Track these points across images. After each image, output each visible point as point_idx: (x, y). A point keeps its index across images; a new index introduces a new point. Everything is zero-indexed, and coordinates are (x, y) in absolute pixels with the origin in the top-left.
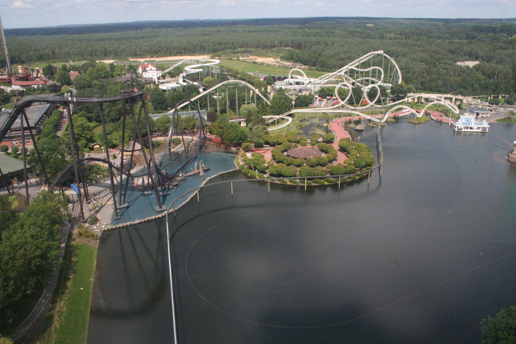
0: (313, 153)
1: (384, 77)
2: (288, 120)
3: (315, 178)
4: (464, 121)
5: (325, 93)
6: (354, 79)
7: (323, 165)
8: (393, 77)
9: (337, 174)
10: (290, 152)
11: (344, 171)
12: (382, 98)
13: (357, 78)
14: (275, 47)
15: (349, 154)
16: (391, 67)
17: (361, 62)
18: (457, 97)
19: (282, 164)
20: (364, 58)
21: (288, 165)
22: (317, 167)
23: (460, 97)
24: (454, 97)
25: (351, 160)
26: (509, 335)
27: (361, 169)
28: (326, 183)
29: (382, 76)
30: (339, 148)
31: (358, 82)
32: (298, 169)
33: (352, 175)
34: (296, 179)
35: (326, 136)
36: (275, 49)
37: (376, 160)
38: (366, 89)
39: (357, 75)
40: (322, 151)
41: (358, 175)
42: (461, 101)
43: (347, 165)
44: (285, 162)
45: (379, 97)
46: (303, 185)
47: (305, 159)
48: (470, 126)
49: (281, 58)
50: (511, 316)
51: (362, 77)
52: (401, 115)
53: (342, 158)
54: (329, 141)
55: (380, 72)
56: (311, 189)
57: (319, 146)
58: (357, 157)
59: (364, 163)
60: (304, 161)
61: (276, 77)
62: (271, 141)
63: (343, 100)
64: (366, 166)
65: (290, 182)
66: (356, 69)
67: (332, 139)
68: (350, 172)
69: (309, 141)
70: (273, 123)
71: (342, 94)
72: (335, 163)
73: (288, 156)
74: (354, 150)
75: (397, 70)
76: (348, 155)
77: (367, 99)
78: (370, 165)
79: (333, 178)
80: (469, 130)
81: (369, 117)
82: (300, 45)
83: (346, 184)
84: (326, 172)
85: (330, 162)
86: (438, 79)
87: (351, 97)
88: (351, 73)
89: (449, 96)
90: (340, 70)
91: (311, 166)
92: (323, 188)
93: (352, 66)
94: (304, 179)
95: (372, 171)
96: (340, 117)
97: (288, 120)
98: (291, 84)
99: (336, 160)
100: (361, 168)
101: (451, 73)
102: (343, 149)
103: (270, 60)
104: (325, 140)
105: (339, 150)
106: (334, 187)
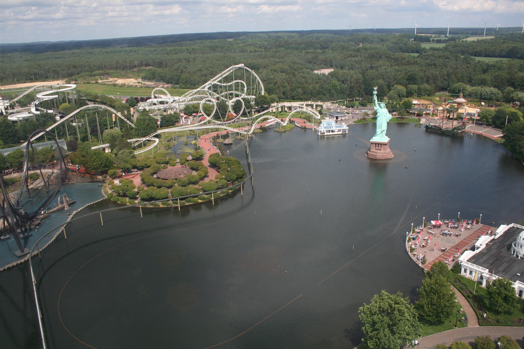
0: (183, 172)
1: (247, 89)
2: (155, 141)
3: (188, 197)
4: (325, 125)
5: (191, 111)
6: (218, 94)
7: (195, 183)
8: (256, 89)
9: (209, 190)
10: (159, 174)
11: (216, 187)
12: (247, 111)
13: (221, 92)
14: (135, 66)
15: (219, 169)
16: (253, 80)
17: (224, 76)
18: (317, 103)
19: (152, 187)
20: (226, 73)
21: (159, 187)
22: (188, 186)
23: (320, 103)
24: (315, 104)
26: (383, 317)
27: (233, 183)
28: (200, 201)
29: (245, 89)
30: (209, 164)
32: (170, 190)
33: (224, 190)
34: (169, 201)
35: (195, 154)
36: (136, 69)
38: (230, 103)
40: (193, 169)
41: (231, 189)
42: (321, 106)
43: (218, 180)
44: (155, 184)
45: (244, 109)
46: (176, 205)
47: (176, 179)
49: (142, 78)
50: (382, 299)
52: (267, 125)
53: (213, 174)
55: (243, 86)
58: (228, 171)
59: (235, 176)
60: (175, 181)
61: (139, 98)
62: (138, 164)
63: (209, 115)
64: (237, 178)
65: (163, 204)
66: (219, 83)
67: (201, 156)
69: (178, 161)
70: (140, 146)
71: (208, 110)
72: (206, 180)
73: (158, 178)
75: (259, 82)
77: (232, 112)
78: (241, 178)
79: (206, 194)
80: (331, 133)
81: (236, 130)
82: (161, 64)
85: (202, 179)
86: (298, 87)
87: (217, 112)
88: (215, 88)
89: (309, 103)
90: (203, 86)
91: (182, 186)
93: (215, 81)
94: (177, 200)
95: (244, 183)
96: (208, 133)
97: (155, 141)
98: (155, 104)
99: (208, 176)
100: (233, 181)
101: (310, 81)
102: (213, 165)
103: (131, 81)
104: (195, 158)
105: (210, 166)
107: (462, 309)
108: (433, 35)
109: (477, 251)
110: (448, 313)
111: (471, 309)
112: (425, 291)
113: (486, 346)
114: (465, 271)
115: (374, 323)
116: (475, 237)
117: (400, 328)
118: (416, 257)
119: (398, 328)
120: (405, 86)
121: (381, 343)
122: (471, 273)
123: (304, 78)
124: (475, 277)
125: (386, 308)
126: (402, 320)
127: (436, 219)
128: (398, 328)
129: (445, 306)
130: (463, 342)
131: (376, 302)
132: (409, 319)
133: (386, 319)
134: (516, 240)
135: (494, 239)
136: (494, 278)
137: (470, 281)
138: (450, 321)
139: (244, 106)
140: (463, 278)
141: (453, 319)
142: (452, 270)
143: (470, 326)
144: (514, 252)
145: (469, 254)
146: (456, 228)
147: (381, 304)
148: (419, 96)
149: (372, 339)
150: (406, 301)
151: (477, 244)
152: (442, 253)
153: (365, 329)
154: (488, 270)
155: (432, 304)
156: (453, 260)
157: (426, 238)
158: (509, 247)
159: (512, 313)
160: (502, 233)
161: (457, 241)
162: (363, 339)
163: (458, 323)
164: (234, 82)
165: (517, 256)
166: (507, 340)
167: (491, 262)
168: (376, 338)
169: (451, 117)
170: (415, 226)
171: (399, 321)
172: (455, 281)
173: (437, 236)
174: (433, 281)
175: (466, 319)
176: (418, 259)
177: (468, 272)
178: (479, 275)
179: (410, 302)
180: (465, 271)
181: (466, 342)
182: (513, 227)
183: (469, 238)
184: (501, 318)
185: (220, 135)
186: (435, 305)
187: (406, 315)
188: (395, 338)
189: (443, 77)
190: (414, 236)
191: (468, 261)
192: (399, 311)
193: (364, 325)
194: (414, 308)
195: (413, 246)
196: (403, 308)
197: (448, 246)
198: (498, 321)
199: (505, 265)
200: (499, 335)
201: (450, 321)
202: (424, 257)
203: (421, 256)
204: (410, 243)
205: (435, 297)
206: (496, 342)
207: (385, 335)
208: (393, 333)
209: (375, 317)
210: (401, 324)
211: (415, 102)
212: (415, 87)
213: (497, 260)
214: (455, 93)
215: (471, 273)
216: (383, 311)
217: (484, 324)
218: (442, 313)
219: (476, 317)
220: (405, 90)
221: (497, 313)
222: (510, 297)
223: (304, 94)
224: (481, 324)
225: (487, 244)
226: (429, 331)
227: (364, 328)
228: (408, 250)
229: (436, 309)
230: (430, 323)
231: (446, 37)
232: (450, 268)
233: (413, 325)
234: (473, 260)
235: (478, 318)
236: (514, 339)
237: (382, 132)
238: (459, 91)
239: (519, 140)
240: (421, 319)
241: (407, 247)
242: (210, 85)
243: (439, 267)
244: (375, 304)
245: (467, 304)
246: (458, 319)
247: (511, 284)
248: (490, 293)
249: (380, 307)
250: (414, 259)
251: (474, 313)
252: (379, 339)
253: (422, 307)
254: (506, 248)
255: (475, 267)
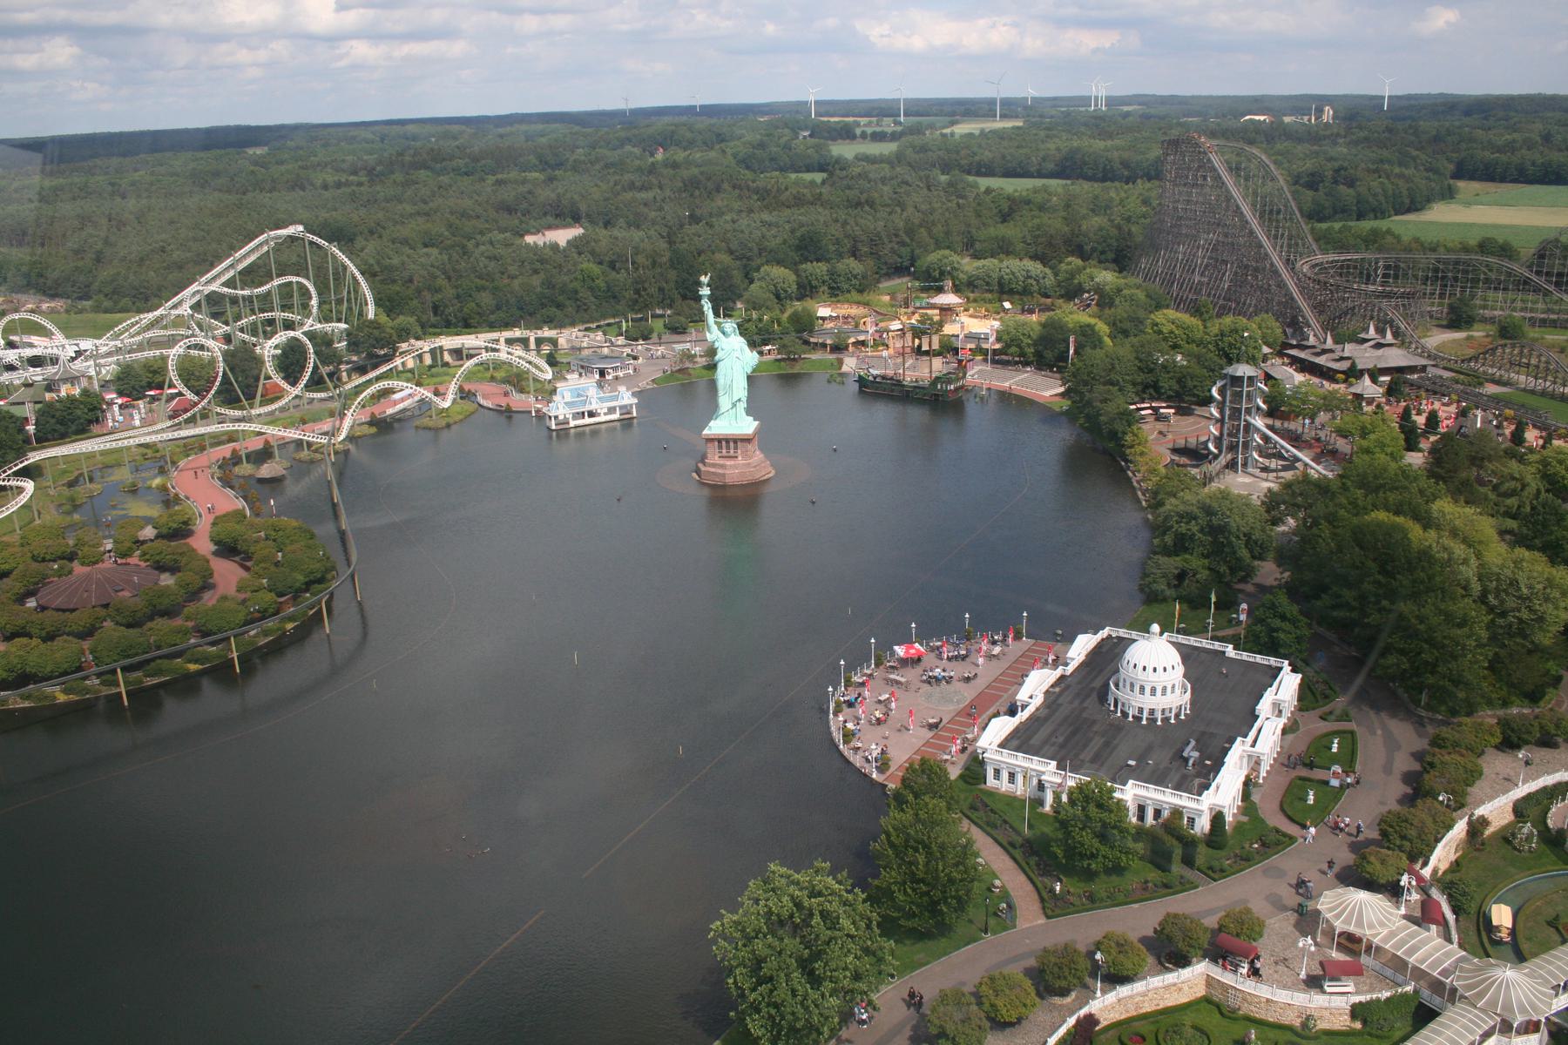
1: (320, 304)
2: (20, 490)
3: (153, 660)
4: (568, 399)
5: (138, 383)
6: (227, 323)
7: (168, 613)
8: (349, 300)
9: (220, 631)
10: (46, 595)
11: (241, 616)
12: (325, 370)
13: (238, 318)
15: (249, 558)
16: (336, 274)
17: (240, 267)
18: (540, 334)
19: (24, 640)
20: (247, 254)
21: (50, 637)
22: (150, 624)
23: (547, 333)
24: (532, 336)
25: (261, 577)
27: (295, 598)
28: (193, 667)
29: (314, 302)
30: (213, 548)
31: (242, 330)
32: (86, 645)
33: (270, 624)
34: (86, 678)
35: (164, 520)
37: (337, 556)
38: (269, 349)
39: (236, 309)
40: (161, 568)
41: (291, 619)
42: (554, 342)
43: (248, 595)
44: (34, 631)
45: (316, 368)
46: (114, 690)
47: (106, 606)
48: (587, 408)
50: (773, 890)
51: (253, 312)
52: (390, 411)
53: (228, 574)
54: (176, 530)
56: (146, 702)
57: (144, 554)
58: (277, 564)
59: (301, 578)
60: (103, 612)
64: (308, 586)
65: (65, 691)
67: (186, 523)
68: (263, 615)
69: (109, 547)
72: (209, 599)
73: (43, 608)
74: (262, 544)
75: (354, 278)
76: (249, 564)
77: (278, 379)
78: (321, 581)
79: (213, 644)
80: (588, 420)
81: (293, 434)
83: (255, 659)
84: (185, 633)
85: (195, 595)
88: (215, 305)
89: (517, 333)
90: (175, 300)
91: (129, 626)
92: (186, 686)
93: (213, 282)
94: (114, 672)
95: (332, 594)
96: (203, 448)
97: (20, 490)
99: (213, 587)
100: (297, 594)
101: (513, 269)
102: (228, 549)
104: (164, 531)
105: (216, 554)
106: (221, 672)
107: (997, 882)
108: (863, 121)
109: (1022, 716)
110: (959, 899)
111: (1023, 878)
112: (892, 845)
113: (1066, 970)
114: (997, 772)
115: (759, 962)
116: (1015, 676)
117: (833, 965)
118: (860, 753)
119: (826, 964)
120: (794, 266)
121: (783, 1018)
122: (1012, 776)
123: (495, 258)
124: (1019, 789)
125: (785, 913)
126: (835, 938)
127: (906, 640)
128: (826, 964)
129: (951, 881)
130: (1006, 971)
131: (757, 901)
132: (853, 932)
133: (791, 944)
134: (1117, 671)
135: (1062, 677)
136: (1071, 783)
137: (1011, 800)
138: (970, 921)
139: (312, 358)
140: (992, 794)
141: (975, 913)
142: (961, 777)
143: (1022, 924)
144: (1116, 706)
145: (1002, 726)
146: (964, 658)
147: (770, 903)
148: (835, 292)
149: (758, 1011)
150: (840, 883)
151: (1022, 695)
152: (931, 734)
153: (735, 983)
154: (1054, 763)
155: (916, 880)
156: (964, 750)
157: (882, 698)
158: (1105, 690)
159: (1124, 869)
160: (1082, 658)
161: (968, 693)
162: (732, 1014)
163: (992, 922)
164: (277, 282)
165: (1125, 714)
166: (1118, 944)
167: (1061, 739)
168: (768, 1005)
169: (925, 348)
170: (851, 668)
171: (828, 943)
172: (973, 808)
173: (913, 688)
174: (908, 817)
175: (1010, 907)
176: (867, 760)
177: (1005, 775)
178: (1035, 781)
179: (854, 886)
180: (997, 772)
181: (1015, 971)
182: (1110, 637)
183: (1001, 681)
184: (1100, 887)
185: (243, 453)
186: (922, 881)
187: (845, 922)
188: (823, 996)
189: (896, 236)
190: (851, 697)
191: (1002, 745)
192: (824, 915)
193: (730, 971)
194: (864, 901)
195: (850, 726)
196: (834, 906)
197: (946, 711)
198: (1092, 898)
199: (1097, 743)
200: (1096, 934)
201: (970, 921)
202: (883, 752)
203: (875, 751)
204: (841, 718)
205: (921, 859)
206: (1091, 954)
207: (794, 992)
208: (815, 981)
209: (759, 945)
210: (835, 948)
211: (823, 312)
212: (820, 269)
213: (1074, 733)
214: (933, 282)
215: (1012, 776)
216: (781, 923)
217: (1058, 911)
218: (946, 903)
219: (1036, 897)
220: (794, 277)
221: (1090, 875)
222: (1115, 827)
223: (498, 308)
224: (1049, 912)
225: (1047, 693)
226: (916, 958)
227: (731, 981)
228: (838, 737)
229: (927, 893)
230: (920, 936)
231: (897, 123)
232: (954, 773)
233: (867, 951)
234: (1015, 743)
235: (1042, 900)
236: (1134, 936)
237: (734, 405)
238: (942, 273)
239: (1105, 401)
240: (889, 927)
241: (833, 729)
242: (197, 298)
243: (924, 775)
244: (753, 904)
245: (1010, 863)
246: (991, 910)
247: (1112, 790)
248: (1064, 824)
249: (770, 913)
250: (857, 760)
251: (1030, 887)
252: (776, 1006)
253: (889, 893)
254: (1094, 695)
255: (1020, 761)
